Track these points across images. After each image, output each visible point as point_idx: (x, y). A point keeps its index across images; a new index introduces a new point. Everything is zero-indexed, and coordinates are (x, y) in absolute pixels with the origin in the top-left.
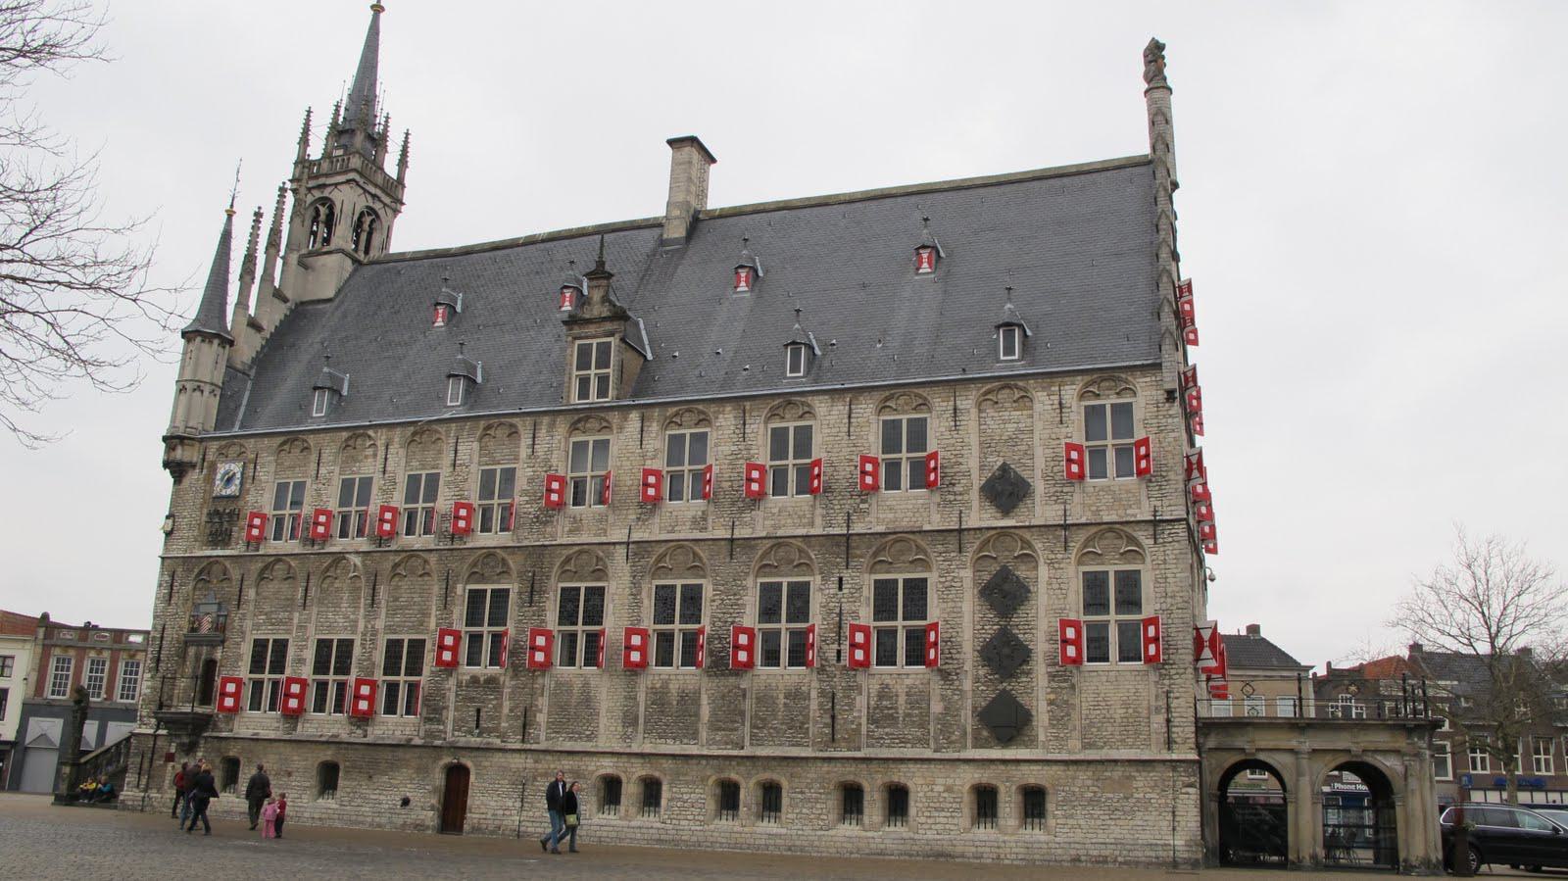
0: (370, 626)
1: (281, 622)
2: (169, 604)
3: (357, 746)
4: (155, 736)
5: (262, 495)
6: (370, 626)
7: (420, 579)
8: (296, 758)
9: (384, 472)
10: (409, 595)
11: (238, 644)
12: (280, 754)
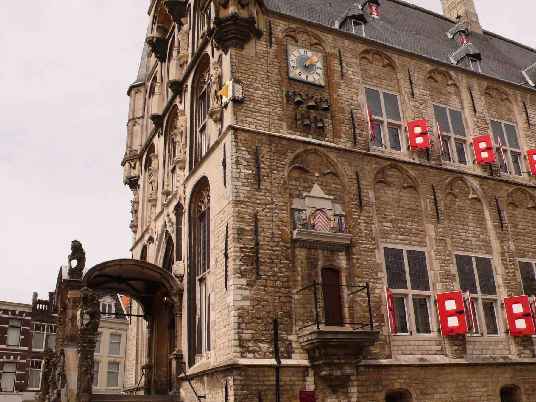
0: (505, 248)
1: (410, 233)
2: (259, 189)
3: (530, 367)
4: (278, 369)
5: (357, 94)
6: (505, 248)
7: (529, 211)
8: (474, 385)
9: (475, 111)
10: (525, 224)
11: (373, 251)
12: (457, 381)
